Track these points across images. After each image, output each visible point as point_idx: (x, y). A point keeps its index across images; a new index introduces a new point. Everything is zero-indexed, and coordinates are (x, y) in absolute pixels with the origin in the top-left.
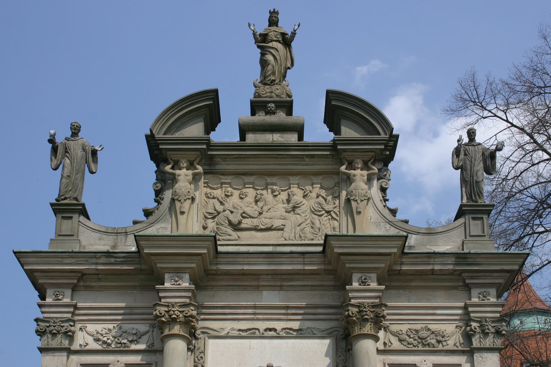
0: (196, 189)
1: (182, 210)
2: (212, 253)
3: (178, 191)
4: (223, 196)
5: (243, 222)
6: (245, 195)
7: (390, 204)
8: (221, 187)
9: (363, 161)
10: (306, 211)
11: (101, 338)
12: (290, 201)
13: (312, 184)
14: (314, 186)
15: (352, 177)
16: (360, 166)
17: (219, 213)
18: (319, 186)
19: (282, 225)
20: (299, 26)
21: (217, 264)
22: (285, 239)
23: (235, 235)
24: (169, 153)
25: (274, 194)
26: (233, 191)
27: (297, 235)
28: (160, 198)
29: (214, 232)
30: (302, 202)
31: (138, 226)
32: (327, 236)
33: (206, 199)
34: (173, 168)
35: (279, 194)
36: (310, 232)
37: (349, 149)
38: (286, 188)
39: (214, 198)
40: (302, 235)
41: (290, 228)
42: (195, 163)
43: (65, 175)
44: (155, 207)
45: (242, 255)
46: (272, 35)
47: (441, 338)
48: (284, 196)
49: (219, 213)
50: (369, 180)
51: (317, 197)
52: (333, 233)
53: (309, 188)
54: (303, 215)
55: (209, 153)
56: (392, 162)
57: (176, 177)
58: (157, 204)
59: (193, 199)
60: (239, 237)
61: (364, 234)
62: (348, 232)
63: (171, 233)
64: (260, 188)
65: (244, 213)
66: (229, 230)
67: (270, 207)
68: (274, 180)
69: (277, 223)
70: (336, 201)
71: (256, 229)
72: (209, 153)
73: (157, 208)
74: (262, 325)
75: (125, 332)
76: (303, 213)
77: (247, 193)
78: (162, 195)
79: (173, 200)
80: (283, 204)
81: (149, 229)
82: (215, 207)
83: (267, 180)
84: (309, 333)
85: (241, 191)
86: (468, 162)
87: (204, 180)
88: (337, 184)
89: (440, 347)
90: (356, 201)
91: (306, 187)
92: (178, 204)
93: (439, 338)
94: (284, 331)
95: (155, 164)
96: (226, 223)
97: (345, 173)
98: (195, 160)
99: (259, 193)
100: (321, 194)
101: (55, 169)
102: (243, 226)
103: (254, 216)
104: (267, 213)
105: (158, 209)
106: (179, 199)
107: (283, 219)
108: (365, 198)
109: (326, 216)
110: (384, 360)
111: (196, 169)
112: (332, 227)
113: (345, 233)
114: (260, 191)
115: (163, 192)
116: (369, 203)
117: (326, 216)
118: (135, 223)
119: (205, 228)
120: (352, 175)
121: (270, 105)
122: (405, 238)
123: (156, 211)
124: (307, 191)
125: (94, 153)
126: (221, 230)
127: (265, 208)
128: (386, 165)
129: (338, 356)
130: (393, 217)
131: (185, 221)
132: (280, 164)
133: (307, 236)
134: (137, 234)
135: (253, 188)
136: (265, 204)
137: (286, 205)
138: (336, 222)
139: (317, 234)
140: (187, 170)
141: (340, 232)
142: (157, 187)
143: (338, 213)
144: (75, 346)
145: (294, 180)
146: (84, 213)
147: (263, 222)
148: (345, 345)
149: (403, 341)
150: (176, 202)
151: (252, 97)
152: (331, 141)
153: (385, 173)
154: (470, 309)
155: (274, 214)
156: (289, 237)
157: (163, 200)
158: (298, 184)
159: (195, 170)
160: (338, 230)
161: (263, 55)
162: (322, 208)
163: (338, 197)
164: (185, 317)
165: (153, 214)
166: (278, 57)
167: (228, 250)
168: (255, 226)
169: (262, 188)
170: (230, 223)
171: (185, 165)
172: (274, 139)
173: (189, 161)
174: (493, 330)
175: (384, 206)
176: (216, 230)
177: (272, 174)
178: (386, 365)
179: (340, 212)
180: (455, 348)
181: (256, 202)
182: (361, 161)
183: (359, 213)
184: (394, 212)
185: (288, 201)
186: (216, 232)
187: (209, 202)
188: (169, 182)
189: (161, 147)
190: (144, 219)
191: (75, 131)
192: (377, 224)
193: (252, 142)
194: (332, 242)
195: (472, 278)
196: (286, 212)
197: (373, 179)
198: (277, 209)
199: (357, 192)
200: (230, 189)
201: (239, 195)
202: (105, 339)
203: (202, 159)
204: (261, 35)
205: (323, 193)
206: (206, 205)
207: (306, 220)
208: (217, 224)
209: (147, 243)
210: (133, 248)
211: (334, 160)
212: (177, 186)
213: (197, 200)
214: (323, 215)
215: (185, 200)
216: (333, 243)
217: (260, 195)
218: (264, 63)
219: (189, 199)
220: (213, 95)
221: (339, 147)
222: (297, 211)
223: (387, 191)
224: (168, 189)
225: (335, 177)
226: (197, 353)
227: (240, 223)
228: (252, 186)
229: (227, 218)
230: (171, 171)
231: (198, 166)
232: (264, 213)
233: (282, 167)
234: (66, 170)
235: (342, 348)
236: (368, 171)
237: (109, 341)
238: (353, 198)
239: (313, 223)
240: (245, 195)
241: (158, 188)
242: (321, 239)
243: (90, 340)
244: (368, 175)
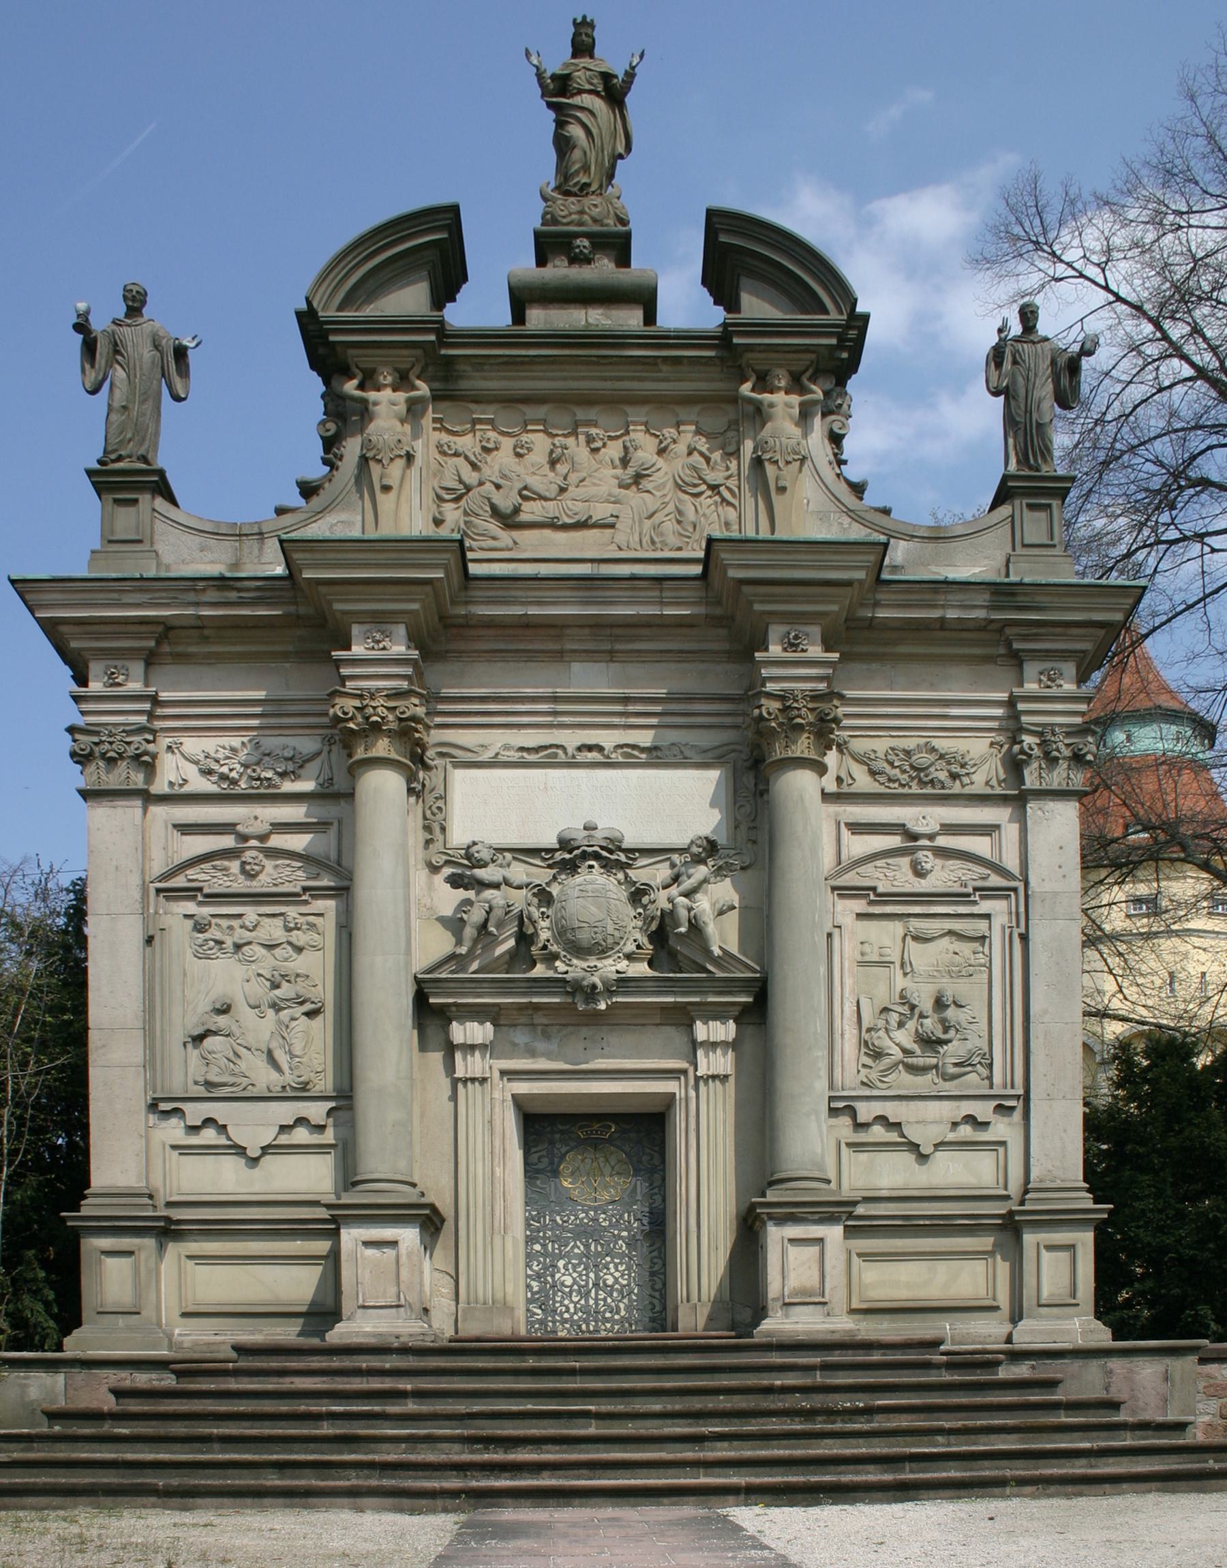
0: (416, 435)
1: (386, 482)
2: (456, 579)
3: (374, 439)
4: (478, 450)
5: (522, 508)
6: (527, 448)
7: (853, 472)
8: (473, 430)
9: (791, 373)
10: (664, 485)
11: (215, 767)
12: (629, 461)
13: (678, 425)
14: (682, 428)
15: (765, 408)
16: (783, 383)
17: (468, 489)
18: (693, 428)
19: (612, 516)
20: (642, 56)
21: (467, 603)
22: (619, 547)
23: (506, 537)
24: (351, 352)
25: (592, 446)
26: (500, 438)
27: (646, 539)
28: (335, 455)
29: (459, 532)
30: (653, 466)
31: (287, 519)
32: (710, 541)
33: (438, 456)
34: (361, 387)
35: (604, 445)
36: (674, 533)
37: (760, 345)
38: (618, 433)
39: (456, 454)
40: (656, 539)
41: (630, 522)
42: (412, 376)
43: (116, 405)
44: (324, 477)
45: (524, 582)
46: (581, 79)
47: (958, 767)
48: (614, 451)
49: (468, 489)
50: (805, 416)
51: (690, 454)
52: (726, 534)
53: (670, 432)
54: (658, 494)
55: (443, 352)
56: (854, 376)
57: (370, 406)
58: (328, 468)
59: (409, 458)
60: (515, 543)
61: (792, 538)
62: (757, 533)
63: (363, 533)
64: (560, 432)
65: (525, 488)
66: (494, 527)
67: (585, 475)
68: (592, 413)
69: (600, 512)
70: (731, 462)
71: (553, 525)
72: (443, 352)
73: (329, 478)
74: (571, 739)
75: (268, 755)
76: (658, 488)
77: (532, 442)
78: (338, 449)
79: (364, 460)
80: (614, 468)
81: (314, 525)
82: (459, 476)
83: (575, 415)
84: (675, 756)
85: (517, 438)
86: (1020, 381)
87: (433, 413)
88: (734, 425)
89: (957, 788)
90: (776, 462)
91: (665, 431)
92: (375, 469)
93: (955, 768)
94: (620, 751)
95: (320, 379)
96: (487, 511)
97: (750, 401)
98: (412, 368)
99: (558, 444)
100: (698, 447)
101: (94, 392)
102: (524, 517)
103: (547, 494)
104: (578, 489)
105: (330, 480)
106: (378, 457)
107: (614, 503)
108: (796, 457)
109: (710, 497)
110: (837, 814)
111: (414, 388)
112: (723, 521)
113: (750, 533)
114: (560, 438)
115: (340, 442)
116: (805, 468)
117: (710, 497)
118: (280, 511)
119: (438, 522)
120: (766, 403)
121: (578, 242)
122: (882, 547)
123: (327, 485)
124: (666, 439)
125: (181, 353)
126: (475, 526)
127: (574, 478)
128: (841, 382)
129: (738, 805)
130: (857, 501)
131: (393, 506)
132: (605, 379)
133: (668, 541)
134: (284, 537)
135: (545, 431)
136: (573, 469)
137: (619, 472)
138: (730, 509)
139: (689, 537)
140: (394, 390)
141: (740, 532)
142: (328, 430)
143: (736, 490)
144: (160, 786)
145: (636, 414)
146: (163, 489)
147: (571, 510)
148: (752, 781)
149: (879, 774)
150: (372, 464)
151: (537, 223)
152: (720, 326)
153: (839, 401)
154: (1021, 706)
155: (593, 490)
156: (628, 542)
157: (341, 460)
158: (646, 424)
159: (412, 390)
160: (736, 527)
161: (560, 124)
162: (700, 478)
163: (736, 454)
164: (400, 720)
165: (321, 491)
166: (595, 131)
167: (492, 572)
168: (553, 518)
169: (566, 432)
170: (496, 512)
171: (389, 379)
172: (591, 321)
173: (396, 370)
174: (1067, 752)
175: (838, 475)
176: (462, 526)
177: (587, 401)
178: (843, 825)
179: (739, 488)
180: (988, 791)
181: (553, 463)
182: (785, 373)
183: (782, 490)
184: (858, 489)
185: (625, 462)
186: (464, 531)
187: (446, 463)
188: (354, 418)
189: (332, 338)
190: (301, 502)
191: (135, 303)
192: (823, 517)
193: (540, 327)
194: (723, 555)
195: (1025, 638)
196: (620, 486)
197: (813, 415)
198: (600, 480)
199: (778, 443)
200: (492, 435)
201: (514, 449)
202: (225, 770)
203: (427, 365)
204: (554, 77)
205: (702, 444)
206: (439, 471)
208: (466, 514)
209: (308, 555)
210: (278, 568)
211: (725, 370)
212: (372, 428)
213: (419, 461)
214: (701, 493)
215: (392, 459)
216: (726, 556)
217: (561, 447)
218: (563, 145)
219: (400, 456)
220: (449, 218)
221: (736, 340)
222: (645, 484)
223: (845, 442)
224: (353, 435)
225: (729, 408)
226: (430, 799)
227: (517, 510)
228: (541, 428)
229: (489, 499)
230: (358, 393)
231: (418, 383)
232: (570, 489)
233: (608, 384)
234: (117, 393)
235: (747, 788)
236: (801, 394)
237: (234, 775)
238: (768, 457)
239: (680, 512)
240: (527, 448)
241: (329, 434)
242: (698, 548)
243: (191, 771)
244: (802, 404)
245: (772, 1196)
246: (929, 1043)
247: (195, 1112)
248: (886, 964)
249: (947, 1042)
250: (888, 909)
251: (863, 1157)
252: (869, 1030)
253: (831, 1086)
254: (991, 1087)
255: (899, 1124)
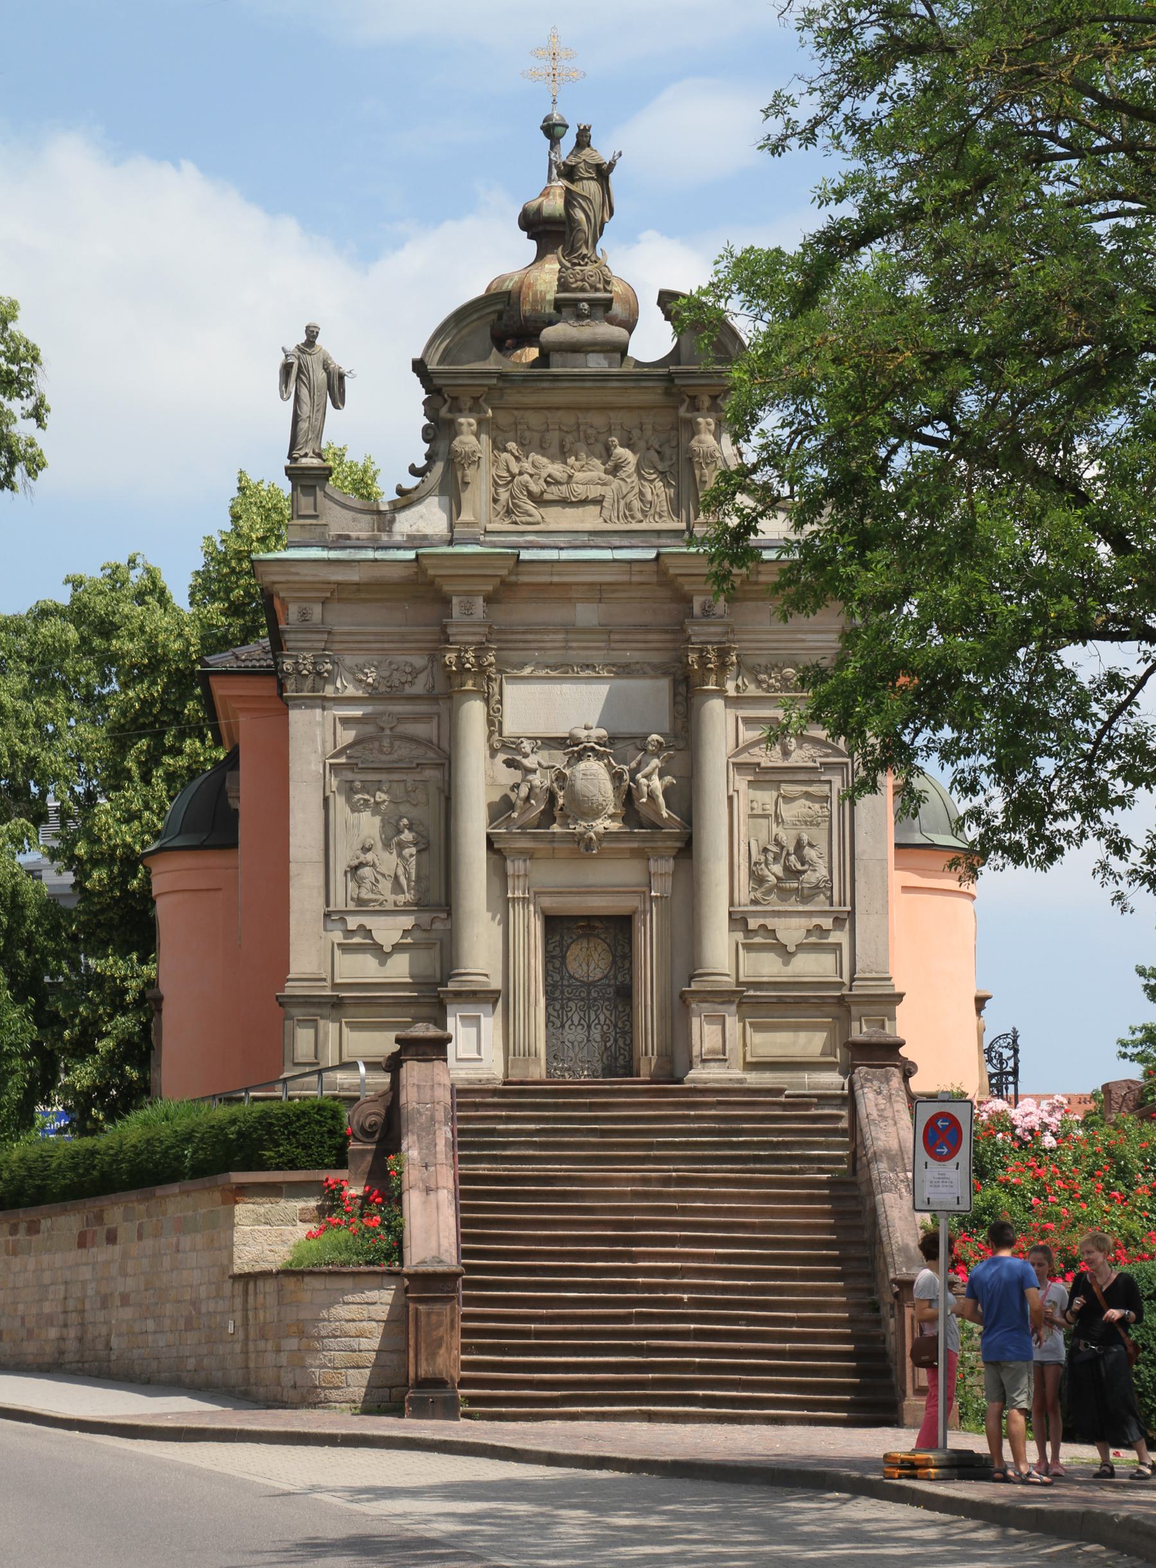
17: (513, 476)
27: (621, 513)
65: (549, 476)
66: (529, 506)
102: (547, 497)
170: (530, 495)
207: (633, 488)
229: (527, 487)
245: (694, 987)
246: (792, 873)
247: (353, 923)
248: (766, 816)
249: (804, 872)
250: (768, 778)
251: (753, 955)
252: (756, 863)
253: (732, 904)
254: (831, 904)
255: (774, 931)
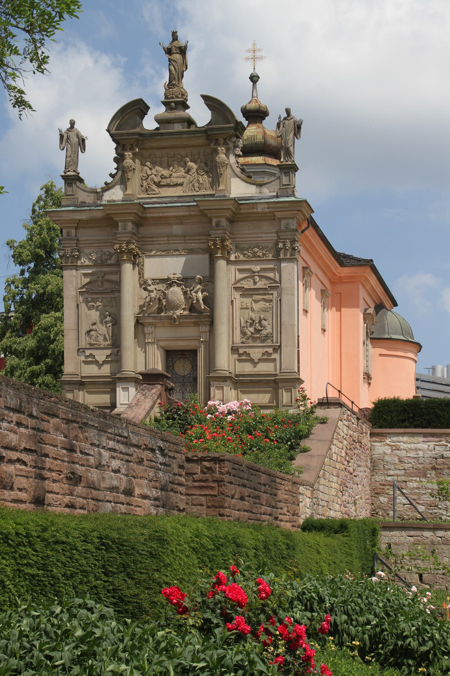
17: (149, 176)
43: (68, 156)
65: (162, 175)
66: (154, 187)
69: (180, 181)
71: (169, 185)
102: (162, 183)
166: (176, 67)
170: (155, 183)
226: (140, 266)
234: (68, 152)
